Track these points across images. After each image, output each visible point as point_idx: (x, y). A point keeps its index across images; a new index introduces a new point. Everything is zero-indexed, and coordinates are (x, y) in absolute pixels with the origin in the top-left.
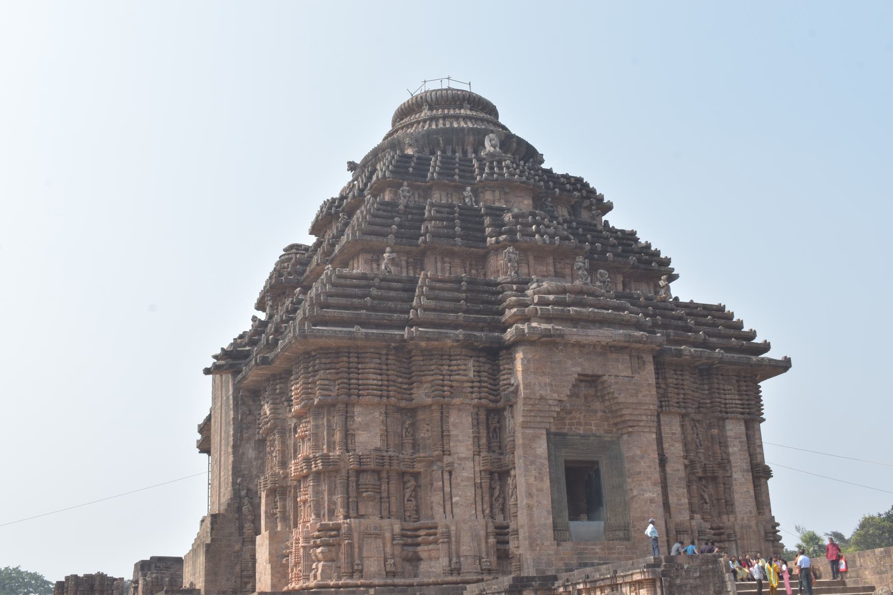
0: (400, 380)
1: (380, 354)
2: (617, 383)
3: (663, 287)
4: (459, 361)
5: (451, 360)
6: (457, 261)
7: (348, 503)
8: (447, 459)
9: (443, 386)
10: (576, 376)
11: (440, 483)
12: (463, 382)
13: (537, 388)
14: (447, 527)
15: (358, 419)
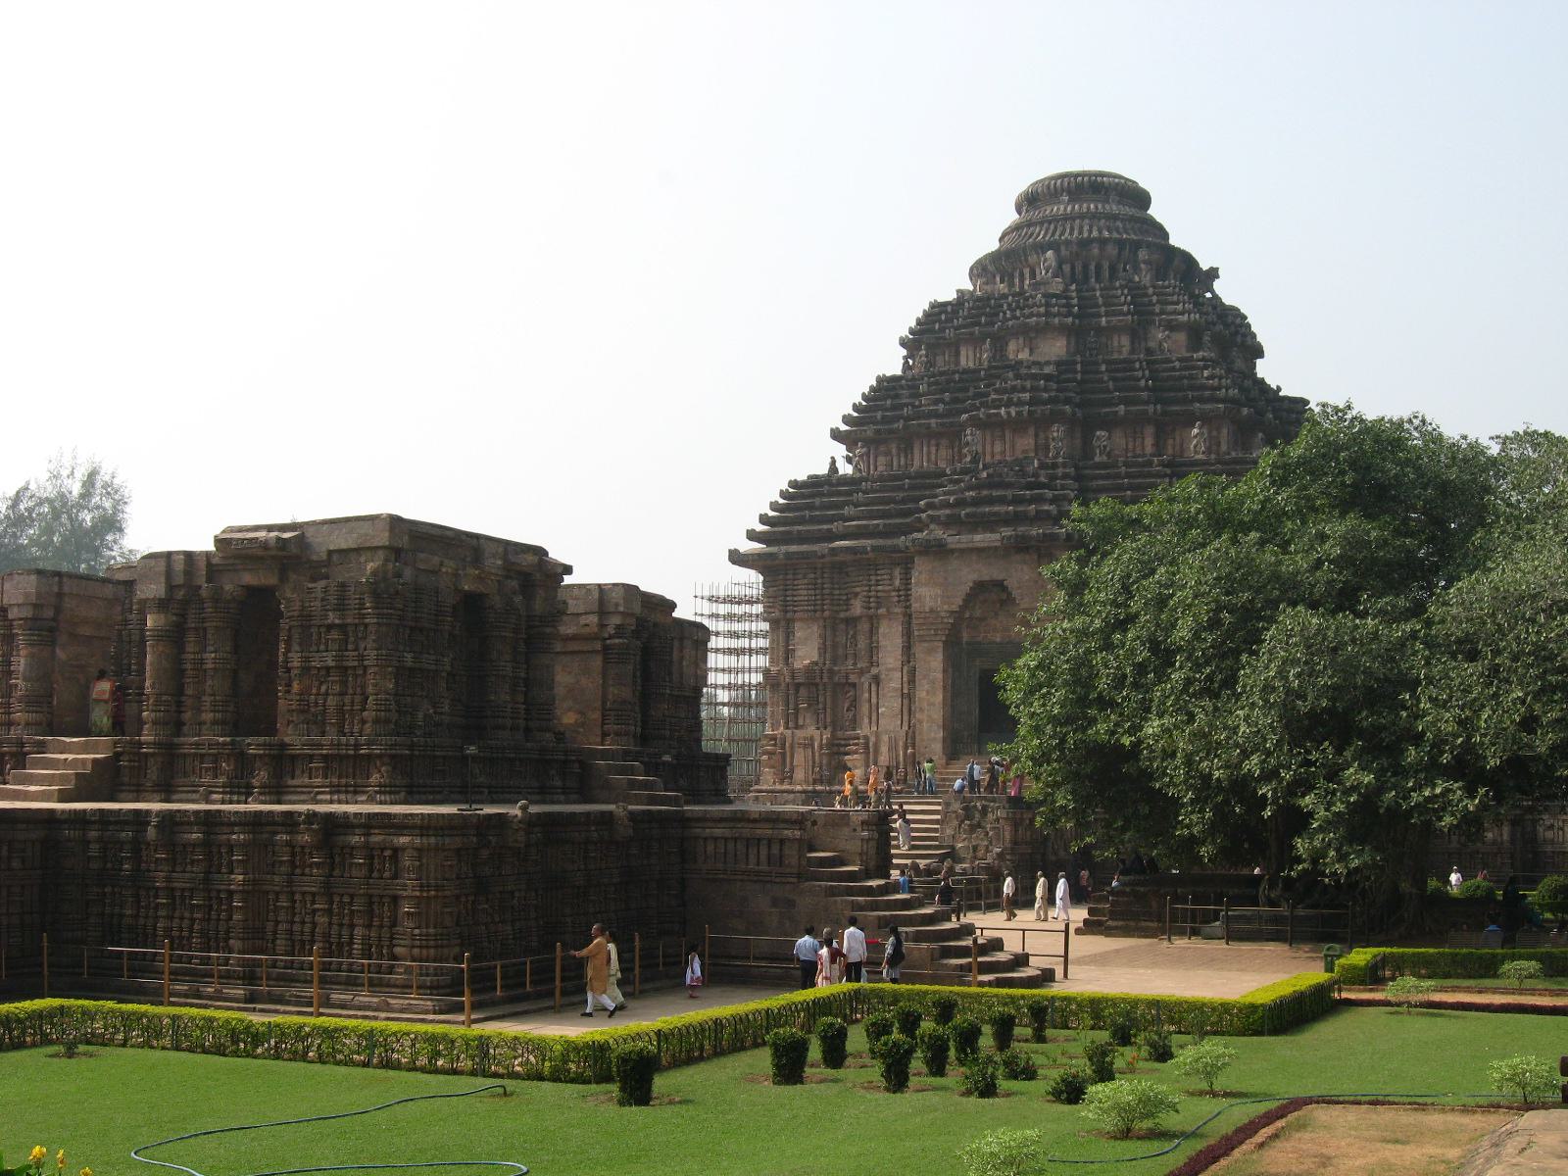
0: (837, 592)
1: (815, 568)
2: (1019, 588)
3: (1196, 437)
4: (883, 572)
5: (877, 570)
6: (944, 442)
7: (788, 714)
8: (874, 671)
9: (870, 597)
10: (971, 585)
11: (866, 695)
12: (889, 591)
13: (928, 599)
14: (866, 738)
15: (798, 634)
